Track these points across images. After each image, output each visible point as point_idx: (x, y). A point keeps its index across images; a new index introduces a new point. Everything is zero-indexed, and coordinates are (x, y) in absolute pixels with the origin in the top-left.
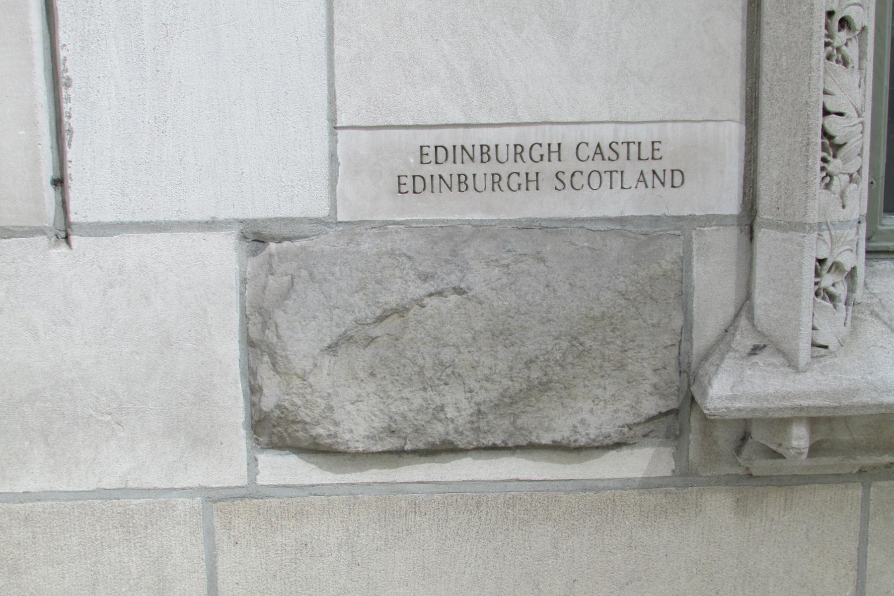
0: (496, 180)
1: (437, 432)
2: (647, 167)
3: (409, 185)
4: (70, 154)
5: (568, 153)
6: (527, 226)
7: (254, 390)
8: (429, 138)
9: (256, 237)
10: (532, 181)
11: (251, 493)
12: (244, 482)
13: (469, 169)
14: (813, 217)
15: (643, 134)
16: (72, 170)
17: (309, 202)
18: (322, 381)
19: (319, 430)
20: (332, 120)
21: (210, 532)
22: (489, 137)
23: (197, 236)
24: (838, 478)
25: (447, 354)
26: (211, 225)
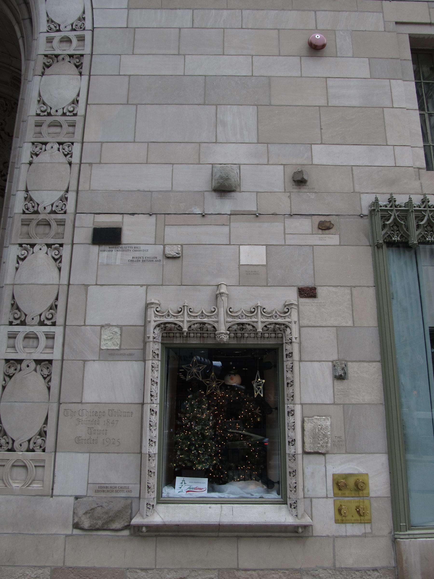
0: (108, 491)
1: (97, 527)
2: (127, 490)
3: (97, 491)
4: (54, 486)
5: (117, 488)
6: (111, 497)
7: (74, 520)
8: (100, 485)
9: (77, 498)
10: (112, 491)
11: (72, 535)
12: (71, 533)
13: (105, 489)
14: (146, 497)
15: (127, 485)
16: (54, 488)
17: (84, 493)
18: (83, 519)
19: (82, 526)
20: (88, 482)
21: (65, 541)
22: (107, 485)
23: (69, 497)
24: (152, 536)
25: (99, 515)
26: (71, 496)
